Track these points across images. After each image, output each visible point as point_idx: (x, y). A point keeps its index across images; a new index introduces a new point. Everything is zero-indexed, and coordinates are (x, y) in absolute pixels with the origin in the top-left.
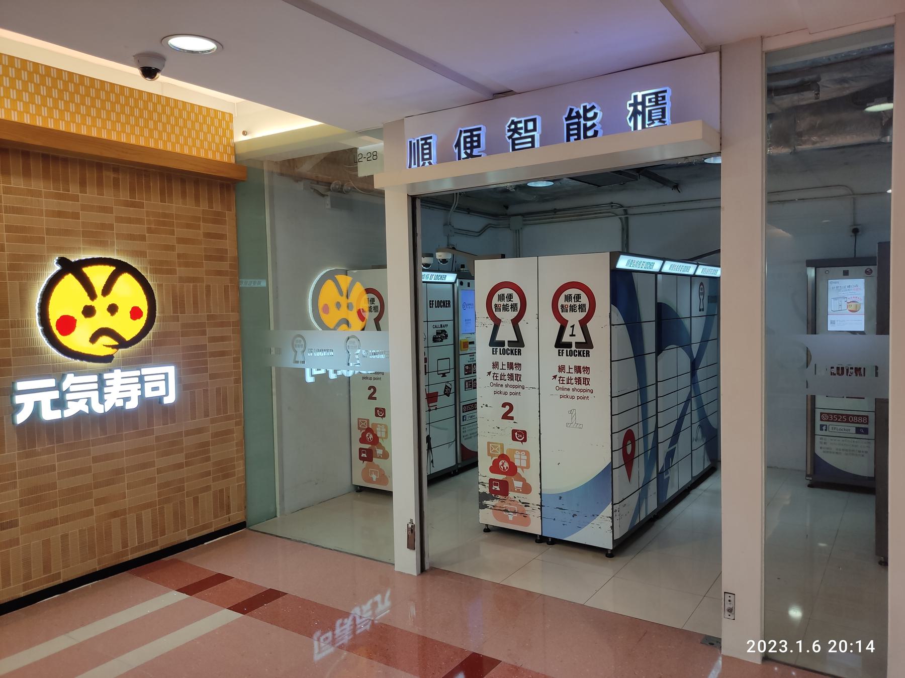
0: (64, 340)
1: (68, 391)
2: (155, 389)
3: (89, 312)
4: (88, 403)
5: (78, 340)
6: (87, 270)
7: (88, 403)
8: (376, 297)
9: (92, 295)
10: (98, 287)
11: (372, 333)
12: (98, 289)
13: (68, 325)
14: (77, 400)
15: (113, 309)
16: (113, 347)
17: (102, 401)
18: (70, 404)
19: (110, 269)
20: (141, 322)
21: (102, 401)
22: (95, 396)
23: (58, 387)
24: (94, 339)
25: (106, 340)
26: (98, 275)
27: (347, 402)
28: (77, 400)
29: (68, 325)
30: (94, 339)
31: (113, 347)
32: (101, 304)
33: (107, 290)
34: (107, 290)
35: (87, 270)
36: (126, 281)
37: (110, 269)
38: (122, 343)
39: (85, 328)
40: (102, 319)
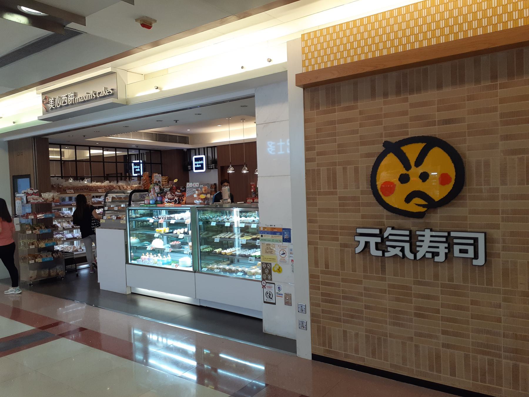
0: (387, 199)
1: (387, 238)
2: (461, 251)
3: (404, 179)
4: (403, 250)
5: (396, 200)
7: (403, 250)
9: (408, 167)
12: (412, 163)
13: (389, 188)
14: (394, 247)
16: (423, 206)
17: (414, 251)
18: (389, 249)
19: (420, 146)
21: (414, 251)
22: (407, 246)
23: (381, 235)
24: (408, 199)
25: (418, 200)
26: (412, 151)
28: (394, 247)
30: (408, 199)
31: (423, 206)
32: (415, 172)
33: (419, 162)
37: (420, 146)
40: (415, 184)
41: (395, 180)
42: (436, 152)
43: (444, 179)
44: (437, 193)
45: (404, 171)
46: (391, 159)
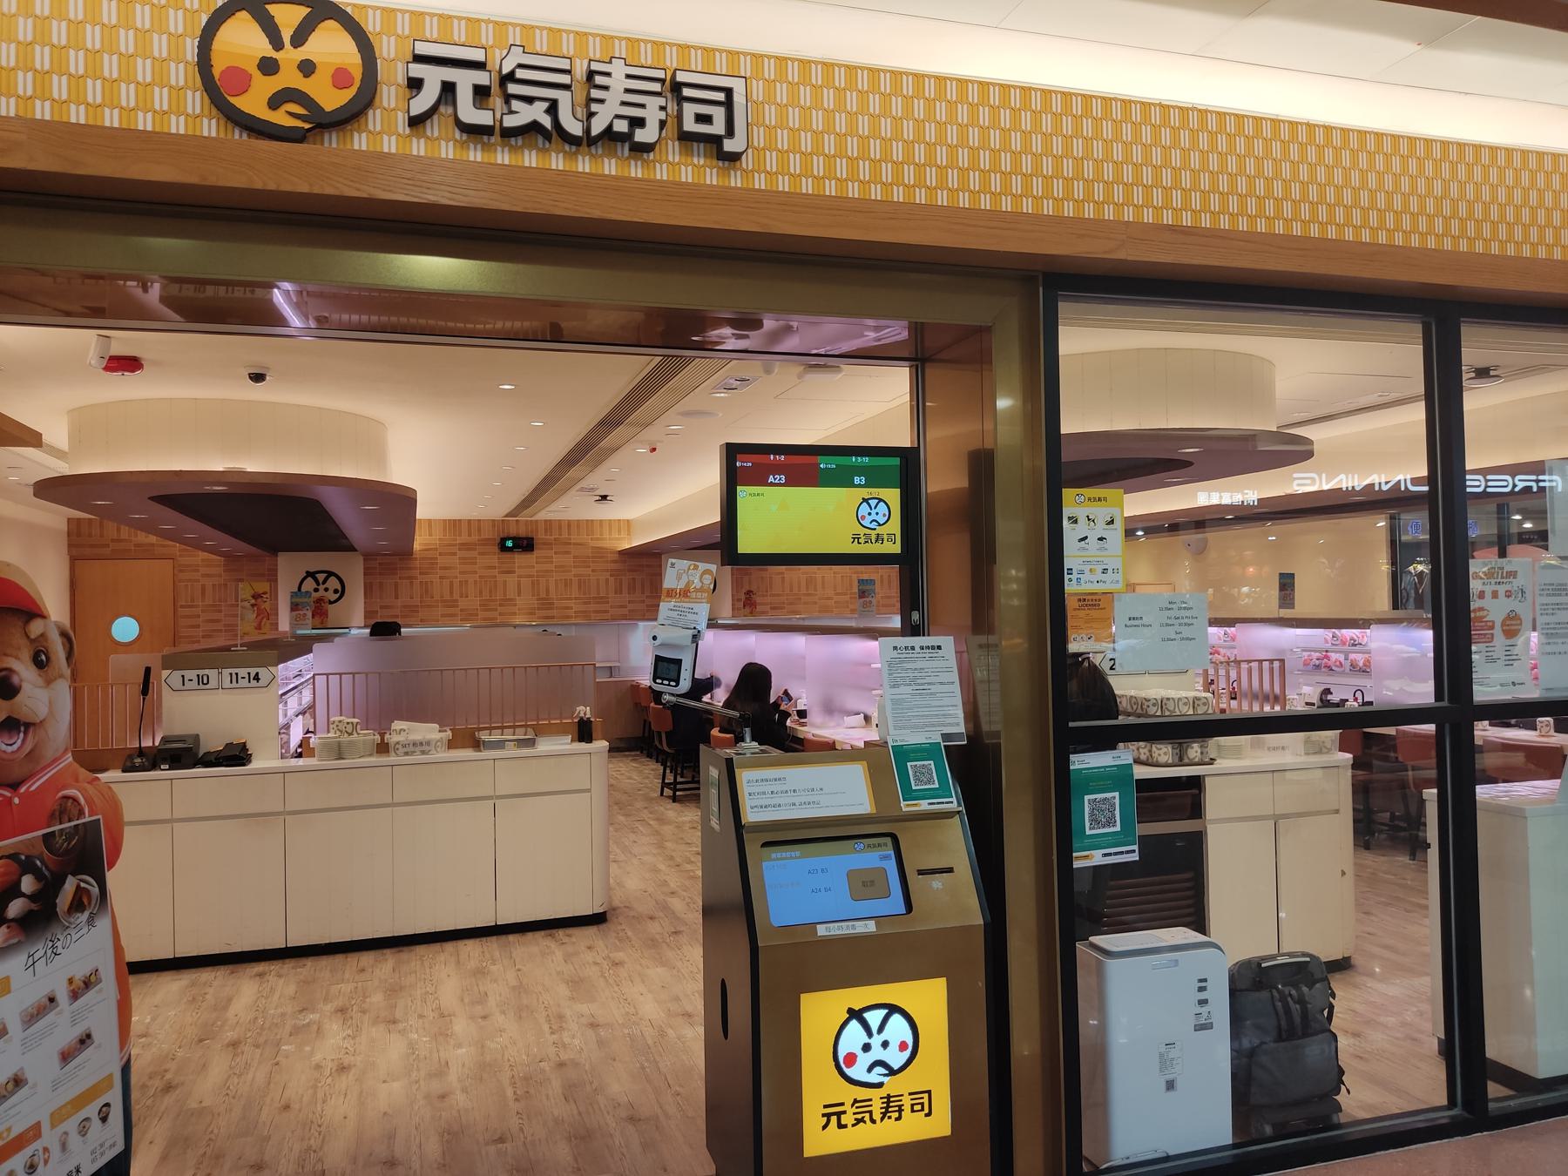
0: (848, 1071)
3: (867, 1048)
6: (867, 1015)
8: (1329, 751)
9: (870, 1034)
10: (874, 1027)
11: (1192, 1022)
12: (875, 1029)
13: (851, 1059)
15: (885, 1044)
19: (884, 1012)
20: (907, 1054)
24: (870, 1070)
26: (874, 1018)
27: (1281, 864)
29: (851, 1059)
30: (870, 1070)
32: (876, 1041)
33: (881, 1029)
34: (881, 1029)
35: (867, 1015)
36: (896, 1019)
37: (884, 1012)
38: (892, 1072)
39: (864, 1060)
41: (858, 1051)
42: (897, 1020)
43: (903, 1046)
44: (896, 1058)
45: (867, 1040)
46: (854, 1025)
